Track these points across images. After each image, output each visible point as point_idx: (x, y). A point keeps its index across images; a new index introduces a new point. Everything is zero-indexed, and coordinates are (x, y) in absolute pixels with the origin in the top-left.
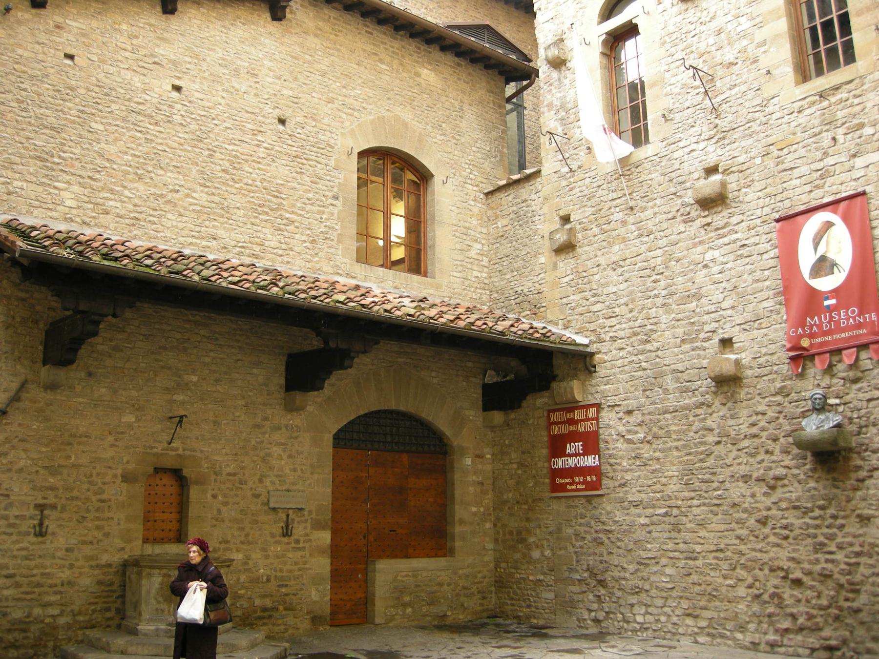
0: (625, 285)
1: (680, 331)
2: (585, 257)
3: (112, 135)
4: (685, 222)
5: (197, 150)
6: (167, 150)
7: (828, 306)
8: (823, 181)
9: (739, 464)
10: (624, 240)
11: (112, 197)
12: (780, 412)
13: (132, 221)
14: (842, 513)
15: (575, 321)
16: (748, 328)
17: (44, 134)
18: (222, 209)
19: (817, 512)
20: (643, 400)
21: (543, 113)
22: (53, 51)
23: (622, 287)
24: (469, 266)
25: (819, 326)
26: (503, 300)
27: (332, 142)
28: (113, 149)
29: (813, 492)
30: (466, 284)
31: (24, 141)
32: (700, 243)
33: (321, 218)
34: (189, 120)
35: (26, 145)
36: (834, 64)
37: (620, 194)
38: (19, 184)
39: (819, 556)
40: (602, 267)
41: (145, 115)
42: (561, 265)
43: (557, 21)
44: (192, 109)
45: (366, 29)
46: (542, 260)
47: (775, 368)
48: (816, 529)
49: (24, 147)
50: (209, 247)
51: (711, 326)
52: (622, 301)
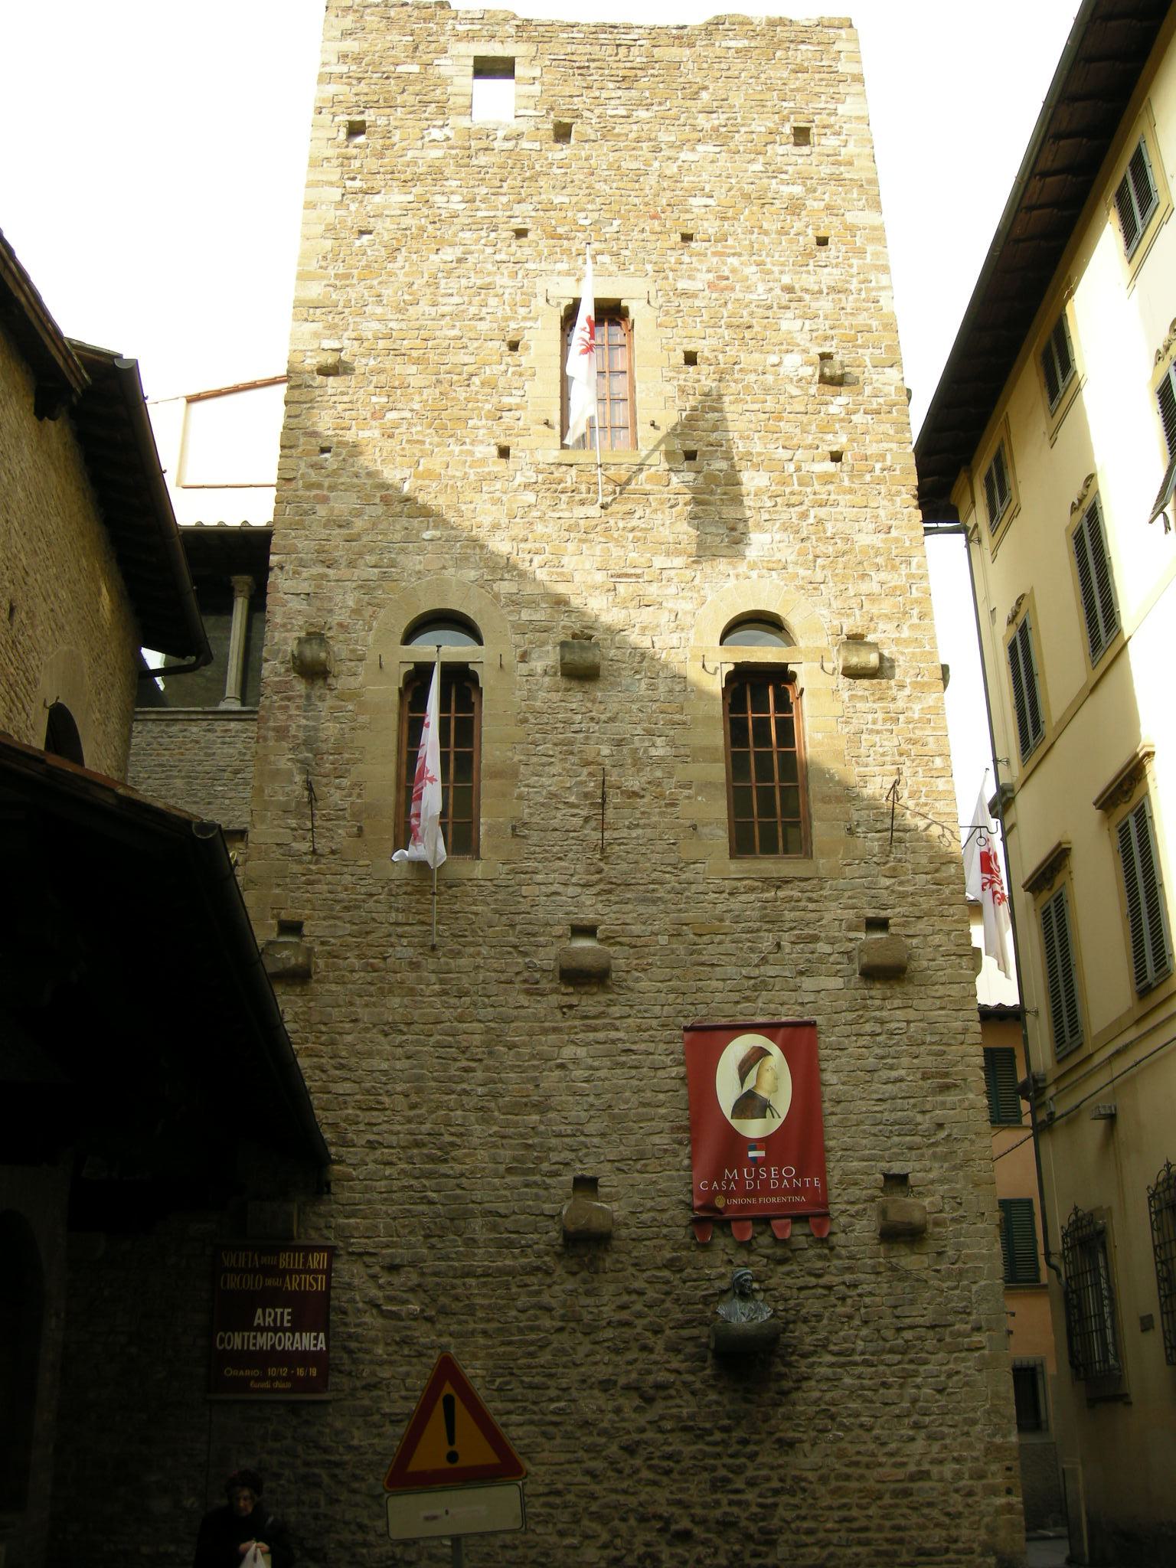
1: (506, 1154)
4: (528, 992)
7: (755, 1159)
8: (756, 994)
9: (596, 1363)
10: (412, 992)
12: (667, 1293)
14: (757, 1437)
16: (625, 1168)
19: (718, 1436)
20: (425, 1251)
23: (399, 1065)
25: (740, 1182)
29: (714, 1408)
32: (555, 1030)
36: (769, 848)
39: (719, 1496)
43: (318, 603)
47: (665, 1231)
48: (715, 1459)
51: (563, 1155)
52: (399, 1089)
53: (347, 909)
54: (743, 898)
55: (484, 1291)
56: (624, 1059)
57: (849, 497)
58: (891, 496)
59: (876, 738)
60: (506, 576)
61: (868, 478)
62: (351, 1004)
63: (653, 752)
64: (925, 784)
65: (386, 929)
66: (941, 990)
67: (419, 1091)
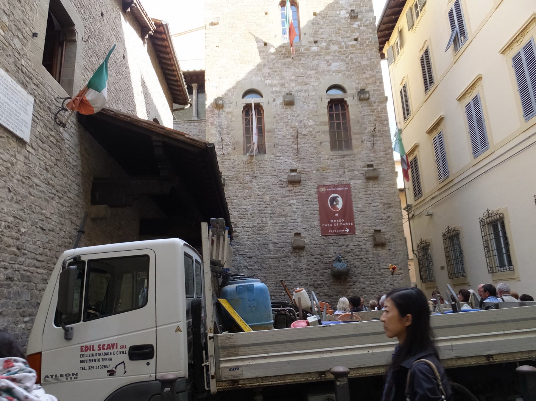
0: (251, 206)
1: (277, 228)
2: (229, 192)
4: (280, 187)
21: (208, 125)
23: (249, 207)
32: (288, 196)
40: (238, 197)
47: (318, 246)
52: (249, 213)
53: (233, 168)
54: (335, 160)
55: (273, 262)
56: (305, 203)
57: (360, 51)
58: (371, 50)
59: (369, 117)
60: (268, 79)
61: (365, 45)
62: (235, 192)
63: (309, 124)
64: (382, 128)
66: (388, 182)
67: (254, 213)
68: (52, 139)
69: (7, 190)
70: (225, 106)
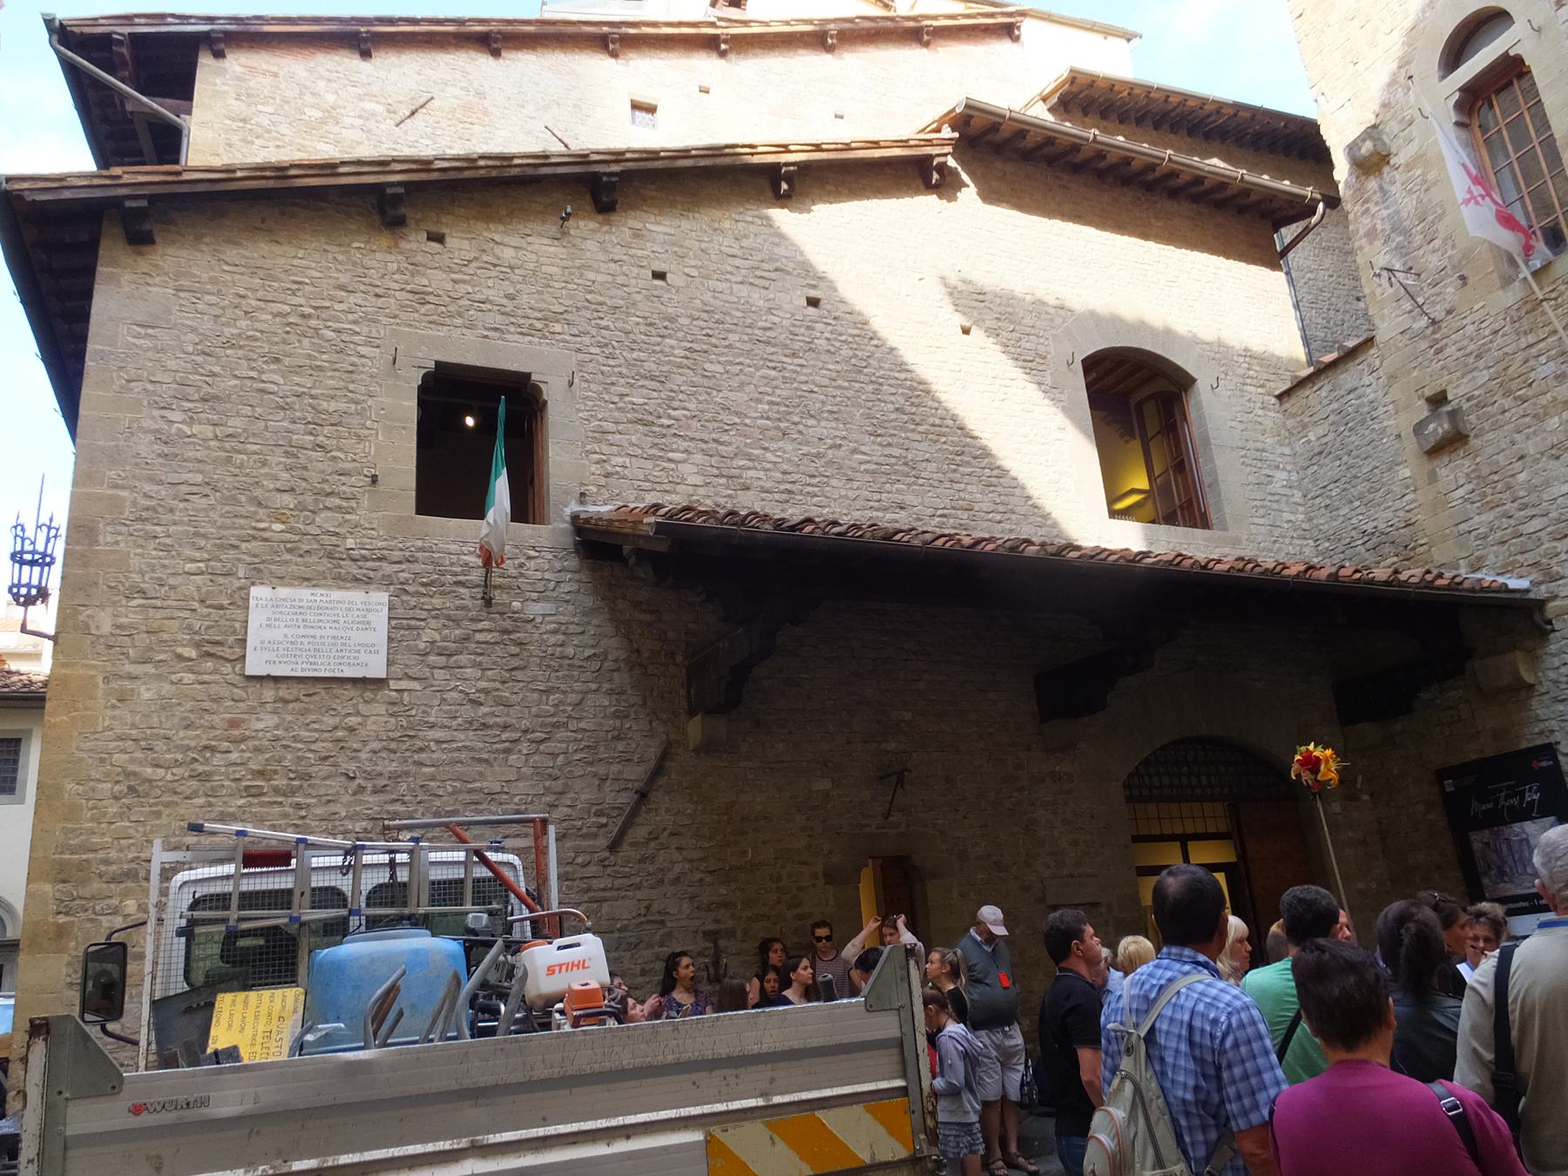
2: (1490, 450)
3: (737, 378)
5: (857, 385)
6: (816, 389)
11: (750, 464)
13: (785, 496)
15: (1492, 556)
17: (642, 386)
18: (906, 464)
21: (1361, 248)
22: (635, 270)
24: (1275, 506)
26: (1343, 548)
27: (1042, 349)
28: (740, 397)
30: (1277, 532)
31: (616, 399)
33: (1047, 461)
34: (838, 344)
35: (620, 405)
37: (1542, 334)
38: (620, 460)
40: (1528, 459)
41: (775, 345)
42: (1442, 472)
44: (840, 329)
45: (1058, 182)
46: (1406, 472)
49: (619, 409)
50: (897, 521)
53: (1479, 357)
65: (1520, 357)
68: (480, 637)
69: (343, 779)
70: (1394, 150)
